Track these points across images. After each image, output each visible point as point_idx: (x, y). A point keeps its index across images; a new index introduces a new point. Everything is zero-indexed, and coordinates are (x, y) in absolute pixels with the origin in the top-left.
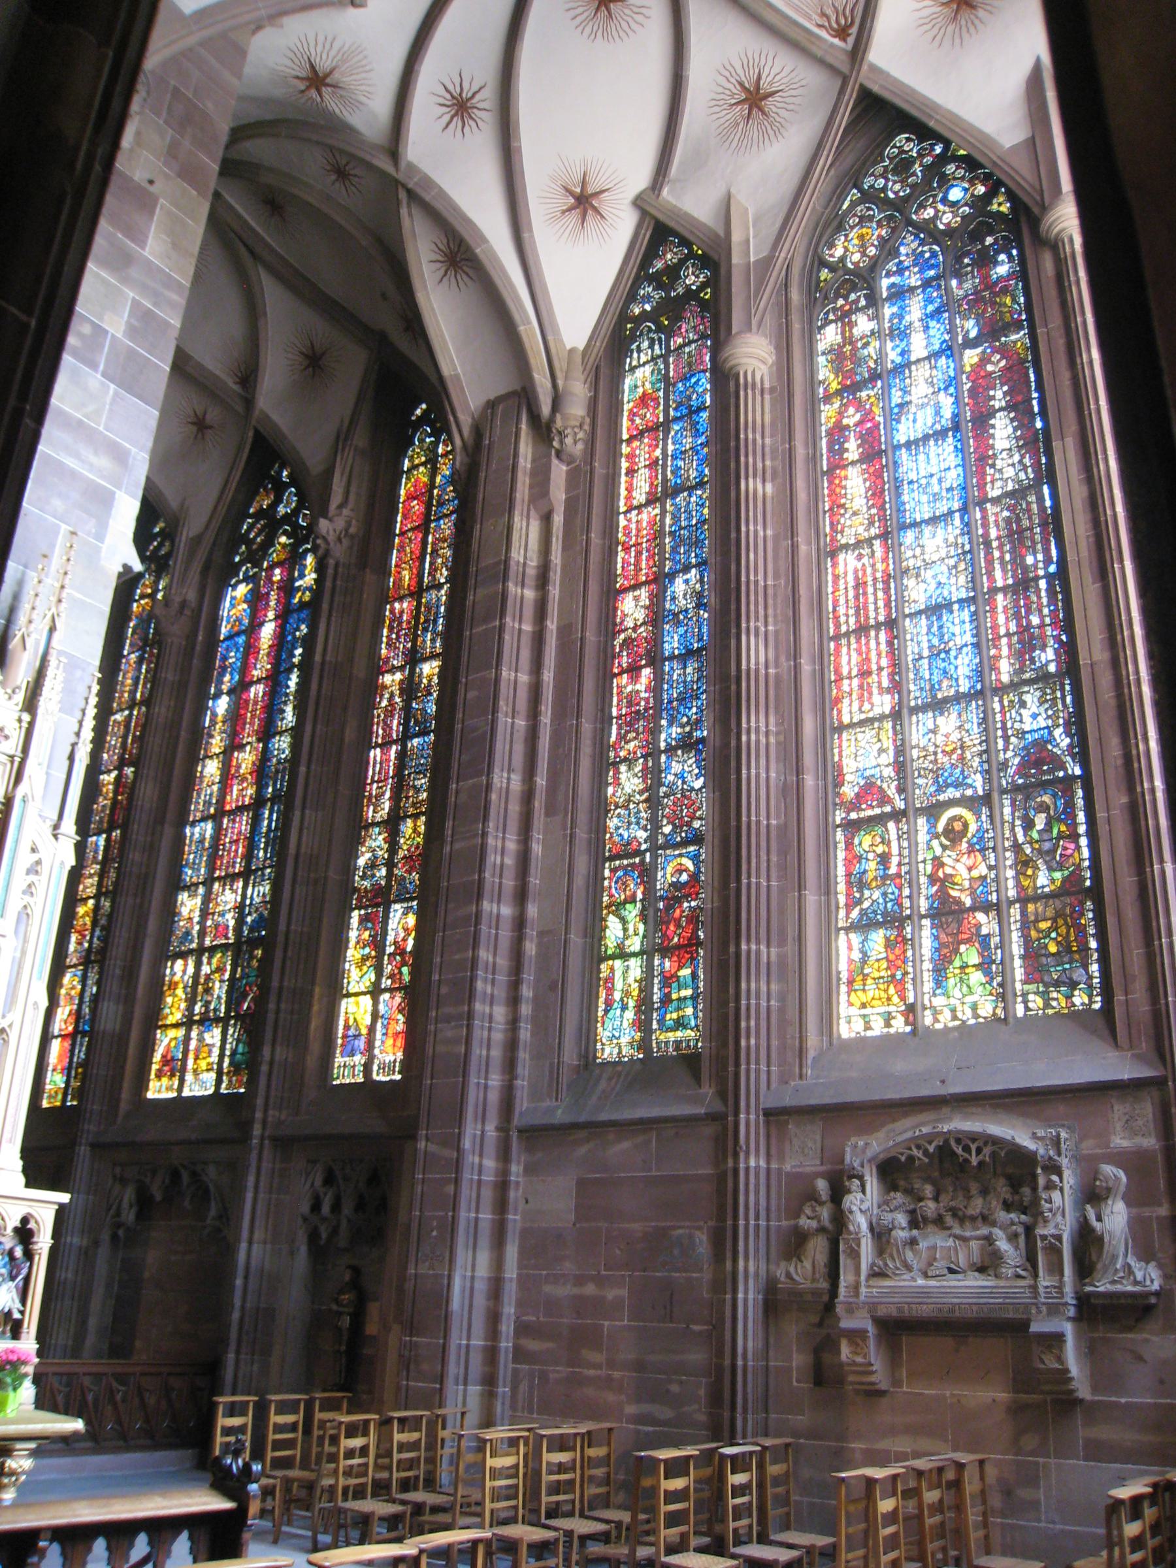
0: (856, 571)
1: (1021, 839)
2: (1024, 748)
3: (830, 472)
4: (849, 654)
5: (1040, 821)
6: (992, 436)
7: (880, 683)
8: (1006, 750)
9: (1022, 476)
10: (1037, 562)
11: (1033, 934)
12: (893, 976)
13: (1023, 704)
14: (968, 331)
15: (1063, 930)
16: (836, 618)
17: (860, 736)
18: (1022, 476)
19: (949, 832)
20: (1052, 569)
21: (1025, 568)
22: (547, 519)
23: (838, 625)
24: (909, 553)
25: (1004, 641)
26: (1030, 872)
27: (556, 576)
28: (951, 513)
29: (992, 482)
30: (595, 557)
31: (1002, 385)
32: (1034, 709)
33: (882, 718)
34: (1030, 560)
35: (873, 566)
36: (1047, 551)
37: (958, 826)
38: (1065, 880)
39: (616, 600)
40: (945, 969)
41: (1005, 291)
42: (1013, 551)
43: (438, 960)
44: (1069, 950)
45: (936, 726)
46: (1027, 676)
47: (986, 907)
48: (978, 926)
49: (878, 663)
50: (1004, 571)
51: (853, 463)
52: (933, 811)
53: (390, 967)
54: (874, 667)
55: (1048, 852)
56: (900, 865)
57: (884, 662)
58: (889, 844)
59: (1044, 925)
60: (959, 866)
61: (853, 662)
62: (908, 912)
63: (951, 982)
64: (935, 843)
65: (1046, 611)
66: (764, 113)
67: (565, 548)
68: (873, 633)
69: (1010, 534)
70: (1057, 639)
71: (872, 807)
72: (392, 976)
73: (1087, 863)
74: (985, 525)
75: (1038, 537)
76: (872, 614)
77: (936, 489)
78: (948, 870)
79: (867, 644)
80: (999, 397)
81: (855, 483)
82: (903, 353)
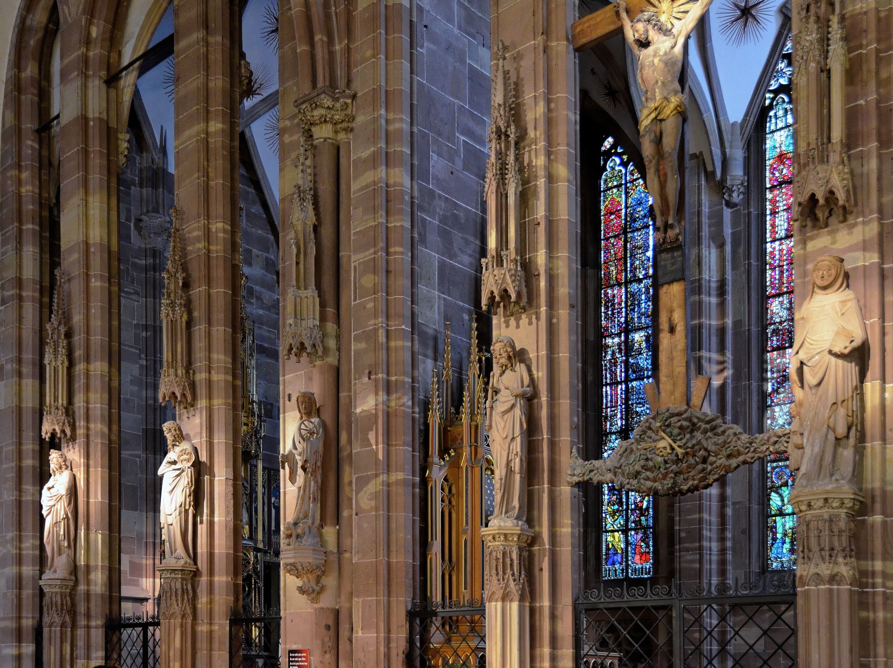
22: (721, 246)
27: (729, 288)
30: (754, 276)
39: (767, 303)
43: (678, 518)
53: (632, 517)
67: (734, 268)
72: (634, 522)
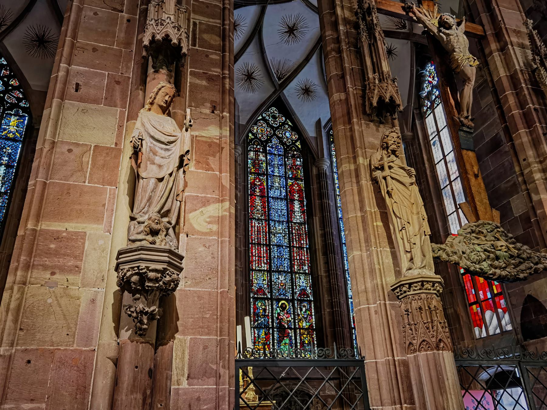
0: (258, 227)
1: (299, 313)
2: (300, 290)
3: (251, 195)
4: (255, 249)
5: (304, 309)
6: (294, 206)
7: (264, 261)
8: (296, 289)
9: (301, 220)
10: (304, 243)
11: (302, 338)
12: (267, 343)
13: (300, 279)
14: (289, 175)
15: (309, 338)
16: (252, 238)
17: (258, 274)
18: (301, 220)
19: (281, 307)
20: (308, 246)
21: (301, 244)
23: (252, 240)
24: (272, 228)
25: (296, 261)
26: (301, 322)
28: (283, 221)
29: (294, 218)
31: (297, 194)
32: (303, 281)
33: (264, 271)
34: (302, 242)
35: (263, 227)
36: (306, 241)
37: (284, 306)
38: (309, 325)
40: (281, 343)
41: (299, 169)
42: (298, 238)
44: (310, 343)
45: (279, 278)
46: (301, 272)
47: (291, 329)
48: (289, 333)
49: (263, 255)
50: (296, 243)
51: (258, 196)
52: (278, 300)
54: (262, 256)
55: (305, 318)
56: (268, 313)
57: (265, 255)
58: (266, 306)
59: (305, 336)
60: (284, 317)
61: (256, 252)
62: (271, 326)
63: (282, 347)
64: (278, 309)
65: (306, 257)
66: (250, 82)
68: (262, 246)
69: (298, 233)
70: (308, 264)
71: (261, 295)
73: (314, 323)
74: (292, 229)
75: (304, 237)
76: (262, 241)
77: (280, 213)
78: (281, 317)
79: (260, 249)
80: (296, 196)
81: (258, 201)
82: (272, 171)
